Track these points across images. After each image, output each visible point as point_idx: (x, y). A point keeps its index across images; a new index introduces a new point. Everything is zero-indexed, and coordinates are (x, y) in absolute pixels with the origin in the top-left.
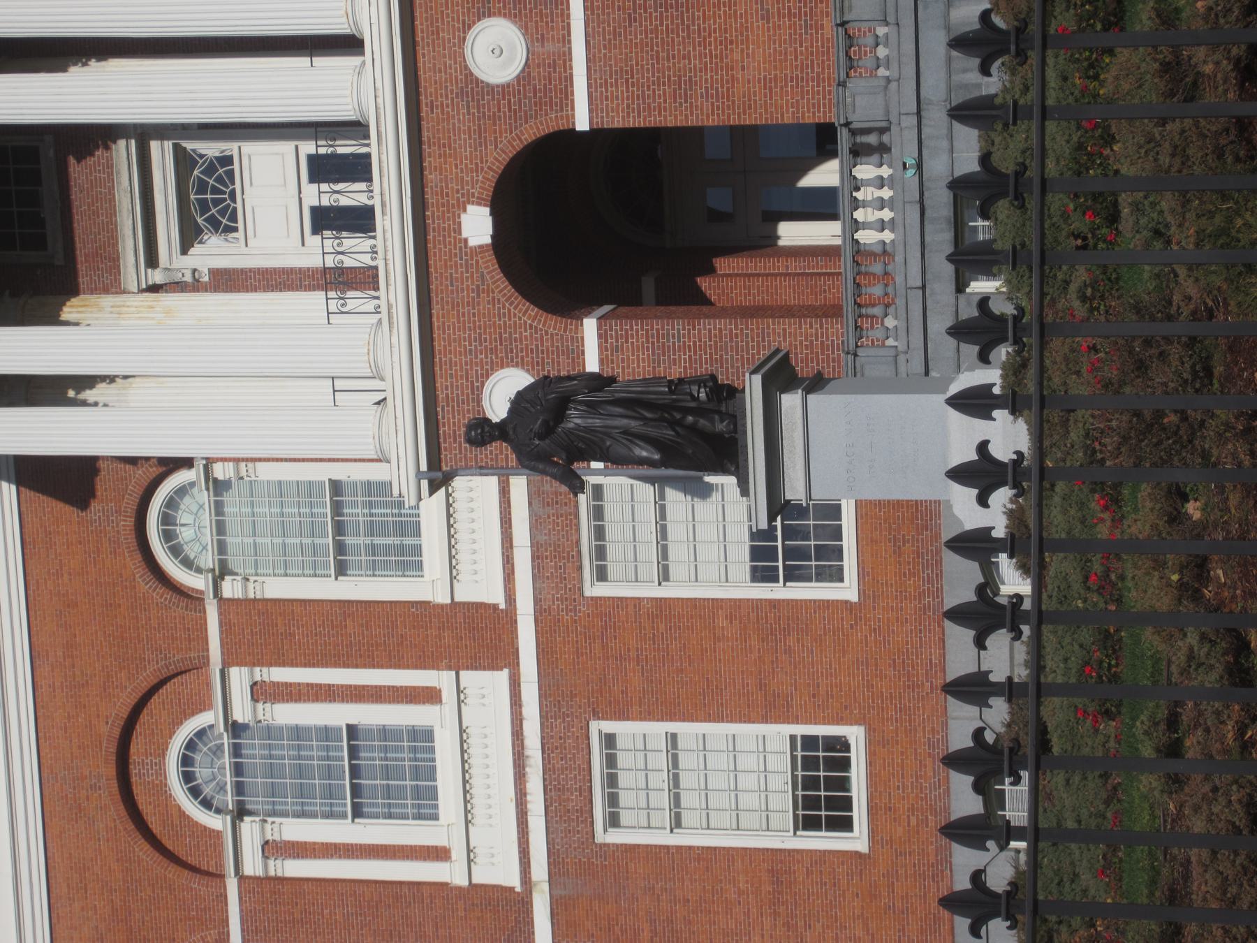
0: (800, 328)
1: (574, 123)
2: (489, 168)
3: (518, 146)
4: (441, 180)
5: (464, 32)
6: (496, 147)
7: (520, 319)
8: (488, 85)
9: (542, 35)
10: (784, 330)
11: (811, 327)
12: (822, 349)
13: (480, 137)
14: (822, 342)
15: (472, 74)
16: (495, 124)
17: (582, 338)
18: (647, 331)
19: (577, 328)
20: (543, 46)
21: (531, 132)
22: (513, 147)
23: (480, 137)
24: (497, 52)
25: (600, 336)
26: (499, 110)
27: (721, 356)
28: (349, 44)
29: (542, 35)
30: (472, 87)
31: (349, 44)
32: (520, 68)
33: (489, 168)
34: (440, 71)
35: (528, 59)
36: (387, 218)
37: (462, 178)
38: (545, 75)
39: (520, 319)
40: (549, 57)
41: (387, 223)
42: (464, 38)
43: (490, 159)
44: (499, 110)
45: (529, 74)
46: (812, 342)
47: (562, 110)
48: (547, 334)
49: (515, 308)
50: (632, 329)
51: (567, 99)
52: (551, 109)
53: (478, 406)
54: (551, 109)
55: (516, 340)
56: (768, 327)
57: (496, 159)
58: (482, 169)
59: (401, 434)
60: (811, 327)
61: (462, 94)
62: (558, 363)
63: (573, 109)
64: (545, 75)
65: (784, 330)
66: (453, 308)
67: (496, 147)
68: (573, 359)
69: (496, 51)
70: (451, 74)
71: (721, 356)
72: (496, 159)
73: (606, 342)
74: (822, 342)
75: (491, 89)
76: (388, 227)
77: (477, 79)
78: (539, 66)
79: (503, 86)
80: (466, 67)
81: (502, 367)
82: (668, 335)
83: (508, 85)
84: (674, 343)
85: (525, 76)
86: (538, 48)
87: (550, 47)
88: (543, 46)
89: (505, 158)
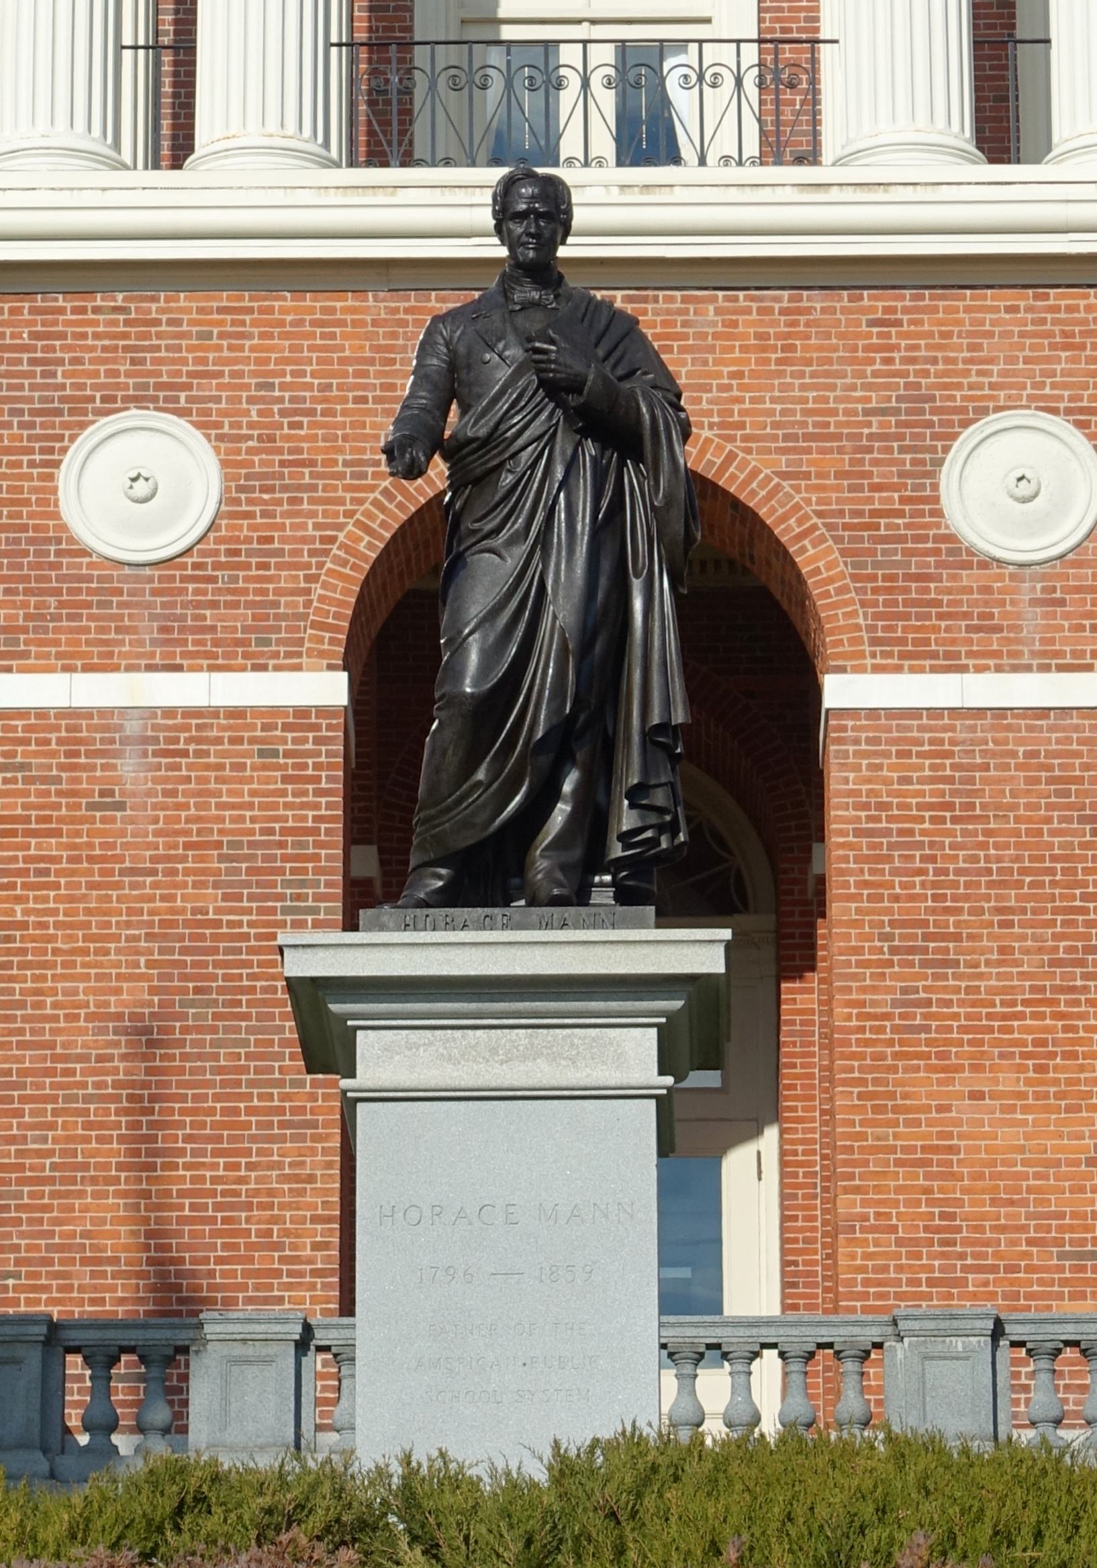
0: (315, 1219)
1: (842, 670)
2: (731, 456)
3: (786, 531)
4: (704, 336)
5: (1069, 411)
6: (784, 476)
7: (349, 514)
8: (940, 463)
9: (1062, 602)
10: (311, 1179)
11: (316, 1246)
12: (258, 1273)
13: (808, 437)
14: (278, 1273)
15: (966, 424)
16: (840, 475)
17: (298, 668)
18: (315, 831)
19: (322, 654)
20: (1034, 602)
21: (819, 562)
22: (784, 518)
23: (808, 437)
24: (1024, 489)
25: (302, 712)
26: (875, 488)
27: (246, 1017)
28: (1002, 121)
29: (1062, 602)
30: (930, 425)
31: (1002, 121)
32: (982, 545)
33: (731, 456)
34: (972, 348)
35: (1000, 562)
36: (615, 195)
37: (707, 388)
38: (950, 602)
39: (349, 514)
40: (1005, 615)
41: (788, 194)
42: (1054, 411)
43: (753, 461)
44: (875, 488)
45: (967, 565)
46: (278, 1246)
47: (874, 642)
48: (308, 579)
49: (375, 503)
50: (319, 793)
51: (903, 656)
52: (876, 616)
53: (127, 399)
54: (876, 616)
55: (293, 501)
56: (316, 1138)
57: (755, 473)
58: (731, 439)
59: (278, 197)
60: (316, 1246)
61: (917, 398)
62: (235, 605)
63: (877, 669)
64: (950, 602)
65: (311, 1179)
66: (377, 349)
67: (784, 476)
68: (245, 643)
69: (1016, 484)
70: (966, 373)
71: (246, 1017)
72: (755, 473)
73: (287, 727)
74: (278, 1273)
75: (929, 471)
76: (402, 196)
77: (954, 437)
78: (987, 590)
79: (936, 500)
80: (984, 412)
81: (224, 464)
82: (303, 884)
83: (938, 513)
84: (281, 897)
85: (957, 554)
86: (1030, 589)
87: (1032, 622)
88: (1034, 602)
89: (754, 497)
